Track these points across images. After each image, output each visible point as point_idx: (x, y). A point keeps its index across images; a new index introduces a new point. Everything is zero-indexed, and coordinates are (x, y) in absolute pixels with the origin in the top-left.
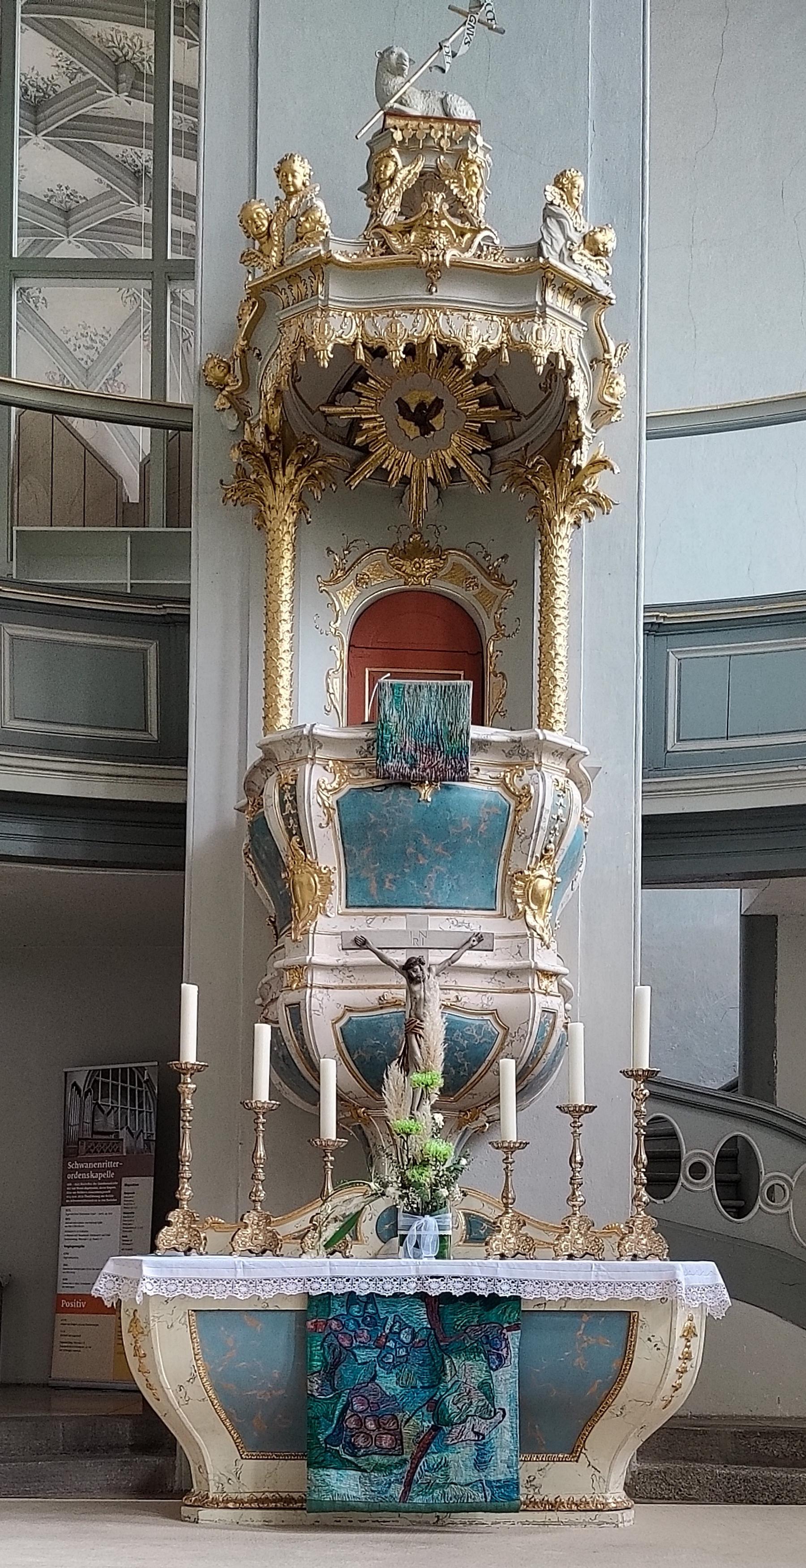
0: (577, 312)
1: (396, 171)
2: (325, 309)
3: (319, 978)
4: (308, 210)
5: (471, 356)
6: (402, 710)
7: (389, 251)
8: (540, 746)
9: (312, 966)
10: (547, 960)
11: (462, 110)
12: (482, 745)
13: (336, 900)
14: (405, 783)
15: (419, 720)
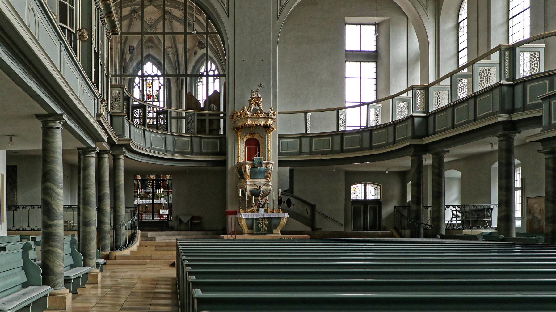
0: (272, 120)
1: (253, 103)
2: (248, 121)
3: (248, 186)
4: (246, 112)
5: (262, 125)
6: (256, 160)
7: (254, 116)
8: (269, 163)
9: (247, 185)
10: (270, 184)
11: (260, 96)
12: (263, 163)
13: (249, 178)
14: (256, 167)
15: (258, 161)
